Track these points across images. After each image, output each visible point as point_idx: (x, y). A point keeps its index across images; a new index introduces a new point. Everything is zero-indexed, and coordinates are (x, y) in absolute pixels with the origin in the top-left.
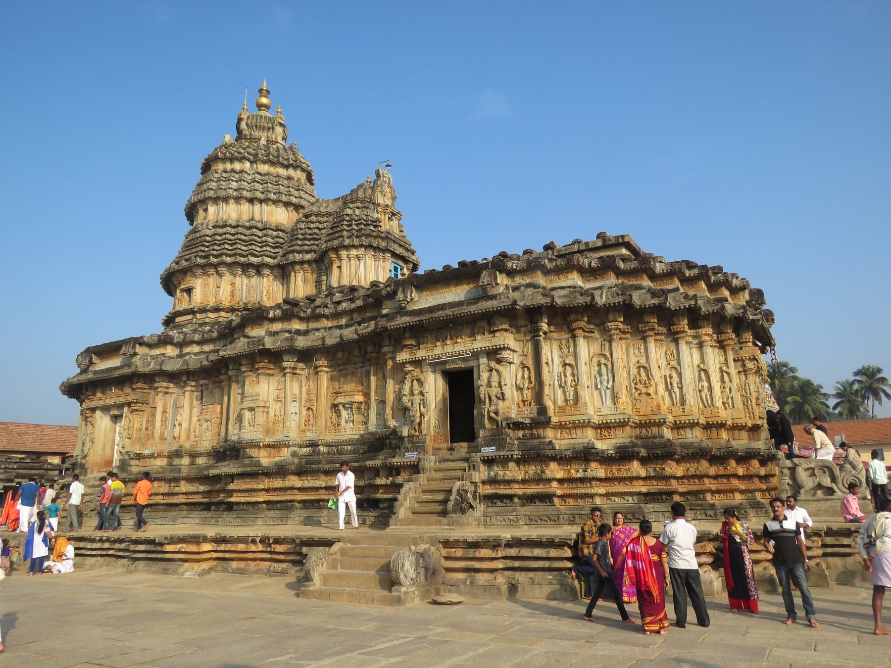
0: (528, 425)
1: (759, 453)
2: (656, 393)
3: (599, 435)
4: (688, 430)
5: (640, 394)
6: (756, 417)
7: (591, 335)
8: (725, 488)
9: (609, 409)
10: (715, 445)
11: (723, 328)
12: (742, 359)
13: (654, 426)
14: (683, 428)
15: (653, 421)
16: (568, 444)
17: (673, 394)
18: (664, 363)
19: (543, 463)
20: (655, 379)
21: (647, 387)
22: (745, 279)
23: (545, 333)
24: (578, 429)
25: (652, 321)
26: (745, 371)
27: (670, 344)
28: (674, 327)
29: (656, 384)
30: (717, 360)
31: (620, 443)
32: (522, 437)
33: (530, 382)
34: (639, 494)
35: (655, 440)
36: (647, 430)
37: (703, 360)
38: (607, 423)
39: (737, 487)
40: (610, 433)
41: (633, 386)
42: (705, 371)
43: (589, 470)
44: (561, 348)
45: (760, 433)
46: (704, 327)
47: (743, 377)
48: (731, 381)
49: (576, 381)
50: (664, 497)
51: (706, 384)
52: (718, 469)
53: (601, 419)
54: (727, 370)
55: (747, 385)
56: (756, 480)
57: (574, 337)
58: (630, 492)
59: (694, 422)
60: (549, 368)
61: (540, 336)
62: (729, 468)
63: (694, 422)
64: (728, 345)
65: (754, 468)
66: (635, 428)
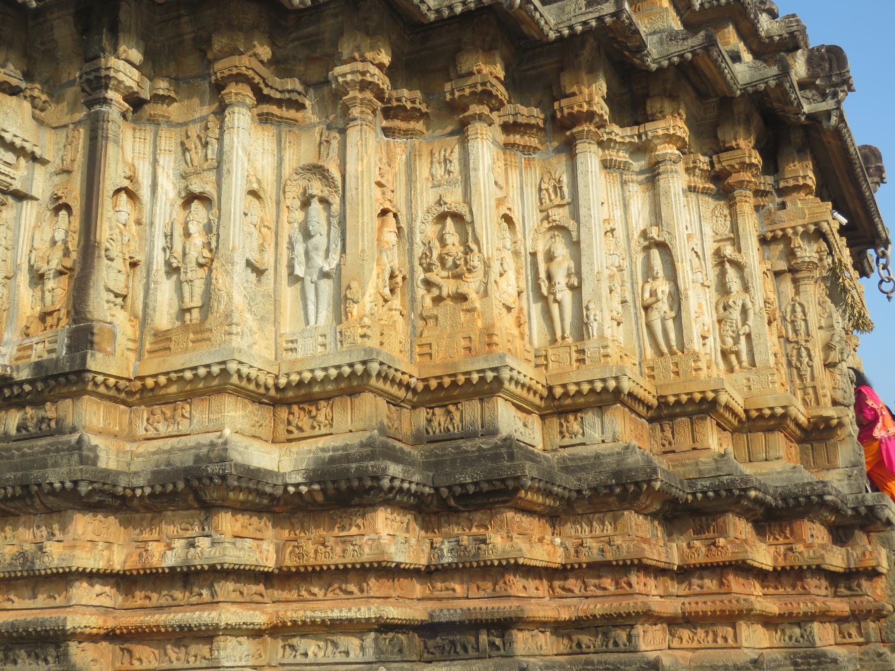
0: (27, 388)
1: (821, 496)
2: (486, 293)
3: (282, 428)
4: (590, 417)
5: (438, 300)
6: (822, 400)
7: (299, 115)
8: (708, 608)
9: (321, 339)
10: (681, 470)
11: (725, 134)
12: (785, 236)
13: (469, 397)
14: (576, 410)
15: (461, 379)
16: (154, 453)
17: (555, 308)
18: (533, 218)
19: (55, 517)
20: (485, 251)
21: (458, 277)
22: (794, 16)
23: (136, 102)
24: (196, 401)
25: (486, 70)
26: (792, 270)
27: (554, 161)
28: (564, 102)
29: (487, 266)
30: (708, 230)
31: (335, 449)
32: (13, 432)
33: (66, 253)
34: (384, 627)
35: (467, 445)
36: (449, 412)
37: (657, 216)
38: (300, 383)
39: (746, 606)
40: (314, 418)
41: (420, 275)
42: (663, 247)
43: (204, 543)
44: (185, 149)
45: (835, 445)
46: (664, 117)
47: (788, 287)
48: (746, 289)
49: (213, 245)
50: (484, 638)
51: (663, 287)
52: (689, 546)
53: (284, 370)
54: (736, 256)
55: (798, 309)
56: (817, 587)
57: (221, 111)
58: (350, 620)
59: (605, 389)
60: (140, 211)
61: (106, 101)
62: (722, 541)
63: (605, 389)
64: (741, 184)
65: (809, 546)
66: (414, 407)
